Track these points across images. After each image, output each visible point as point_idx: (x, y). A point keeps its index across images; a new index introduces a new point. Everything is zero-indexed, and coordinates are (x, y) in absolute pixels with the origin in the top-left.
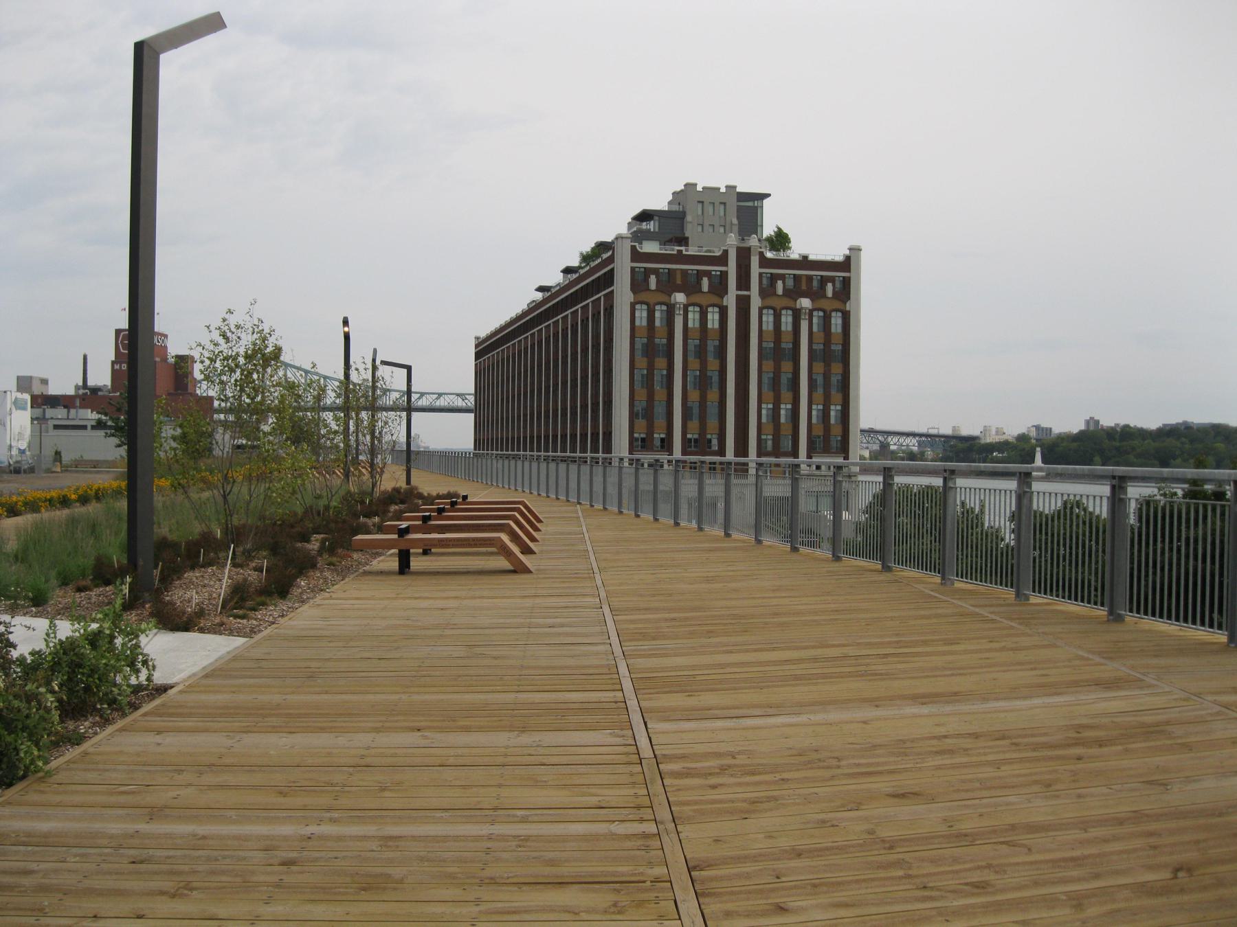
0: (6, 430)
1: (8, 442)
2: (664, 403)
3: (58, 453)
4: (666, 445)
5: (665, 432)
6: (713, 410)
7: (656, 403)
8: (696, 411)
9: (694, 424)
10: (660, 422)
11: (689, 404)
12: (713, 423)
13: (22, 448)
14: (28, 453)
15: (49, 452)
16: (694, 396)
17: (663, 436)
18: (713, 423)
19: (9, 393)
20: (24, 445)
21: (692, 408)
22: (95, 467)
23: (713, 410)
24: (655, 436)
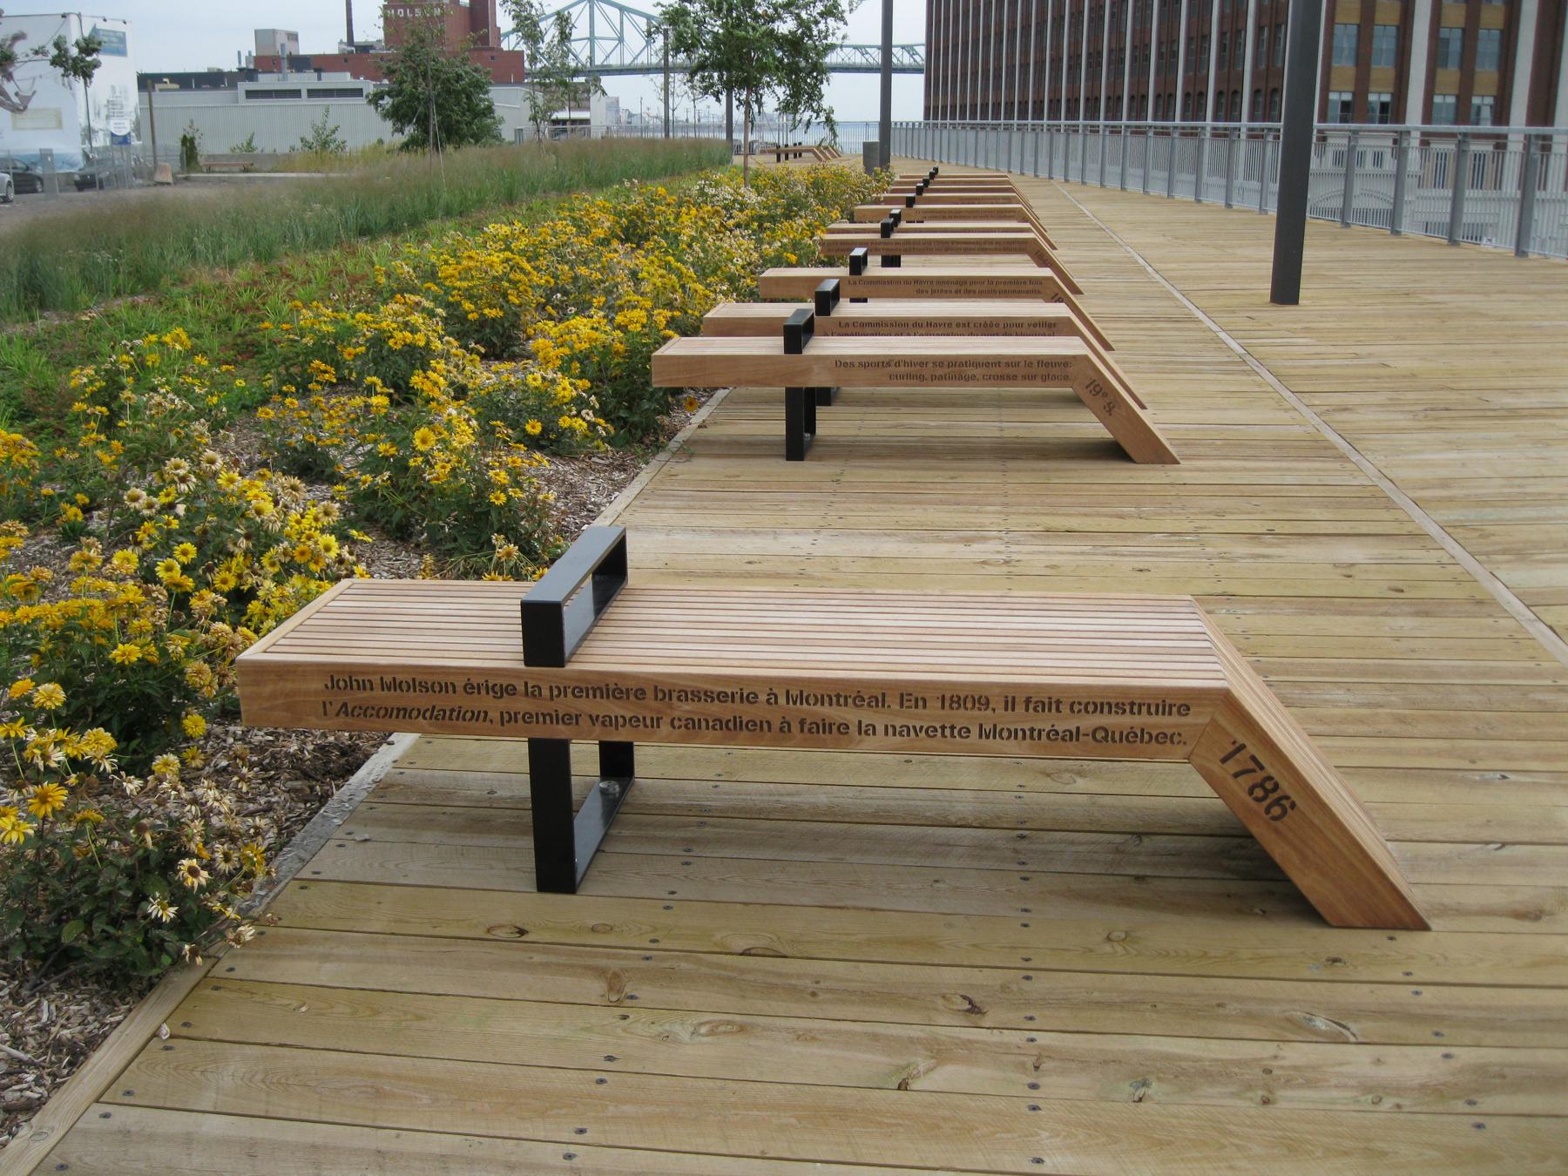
0: (74, 95)
1: (84, 122)
2: (1392, 31)
3: (188, 144)
4: (1393, 111)
5: (1391, 89)
6: (1488, 44)
7: (1378, 30)
8: (1455, 47)
9: (1450, 75)
10: (1382, 69)
11: (1444, 33)
12: (1487, 72)
13: (123, 132)
14: (135, 142)
15: (171, 142)
16: (1455, 15)
17: (1386, 98)
18: (1487, 72)
19: (74, 20)
20: (124, 127)
21: (1447, 41)
22: (246, 170)
23: (1488, 44)
24: (1372, 98)
